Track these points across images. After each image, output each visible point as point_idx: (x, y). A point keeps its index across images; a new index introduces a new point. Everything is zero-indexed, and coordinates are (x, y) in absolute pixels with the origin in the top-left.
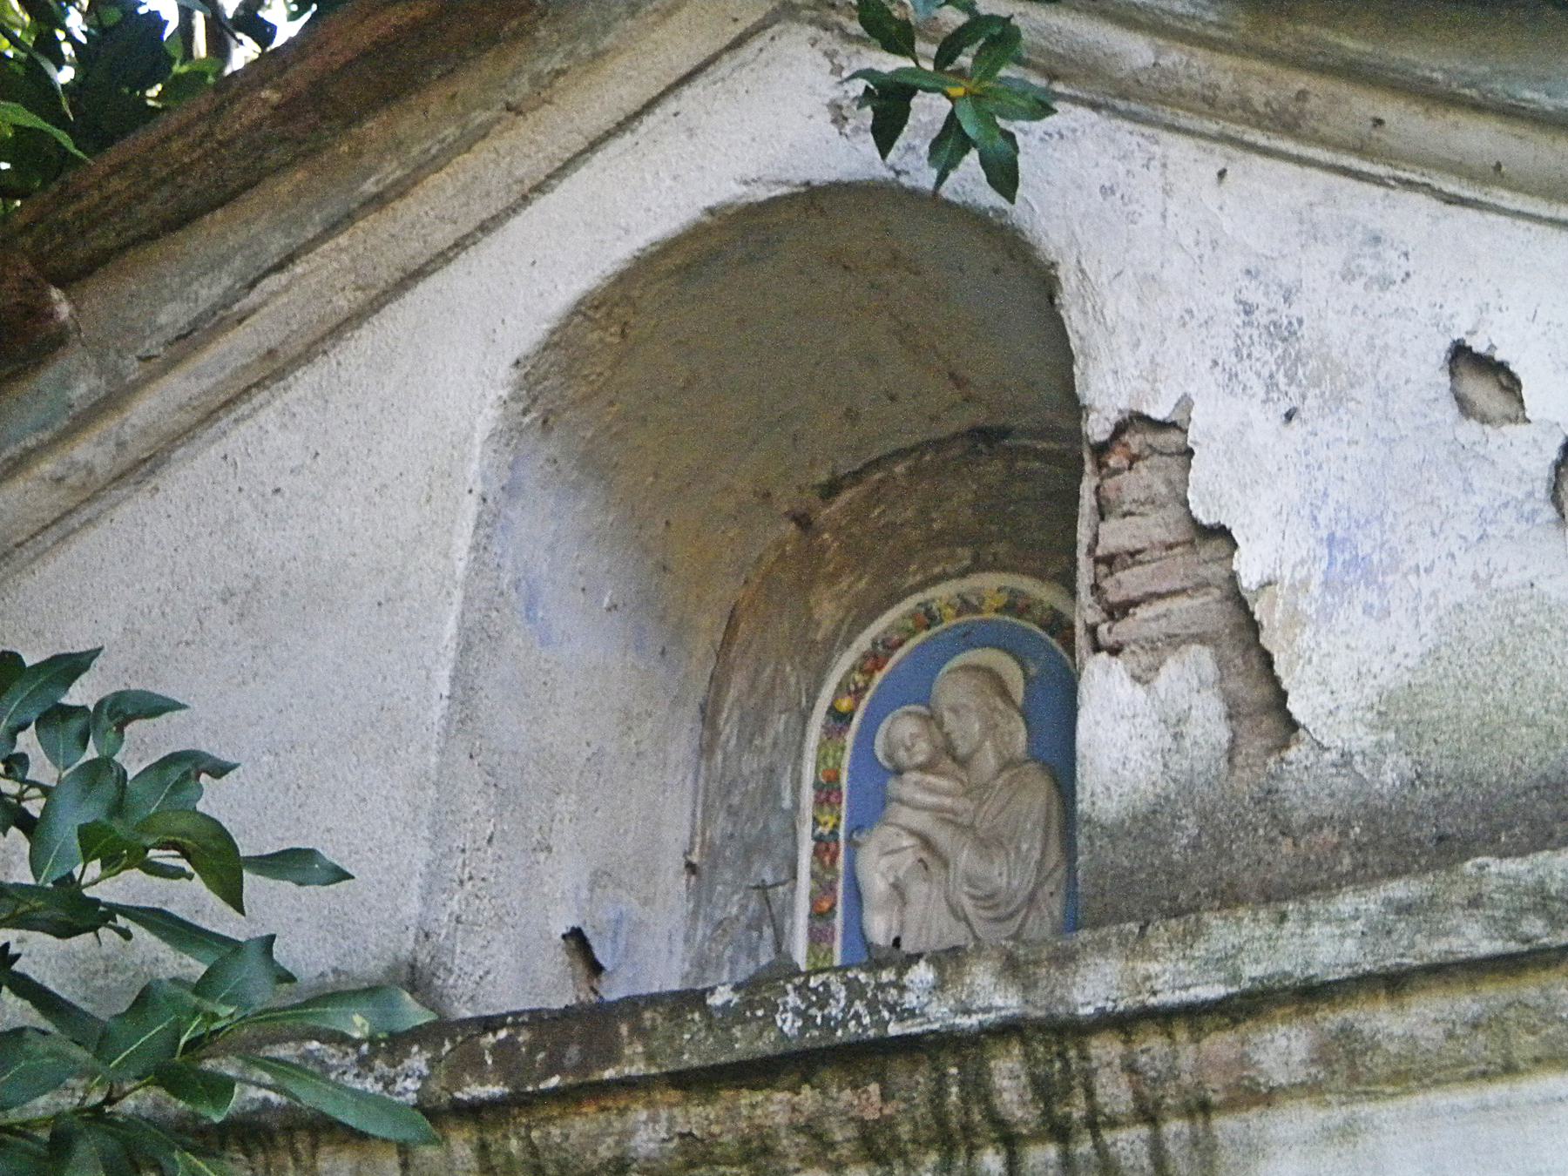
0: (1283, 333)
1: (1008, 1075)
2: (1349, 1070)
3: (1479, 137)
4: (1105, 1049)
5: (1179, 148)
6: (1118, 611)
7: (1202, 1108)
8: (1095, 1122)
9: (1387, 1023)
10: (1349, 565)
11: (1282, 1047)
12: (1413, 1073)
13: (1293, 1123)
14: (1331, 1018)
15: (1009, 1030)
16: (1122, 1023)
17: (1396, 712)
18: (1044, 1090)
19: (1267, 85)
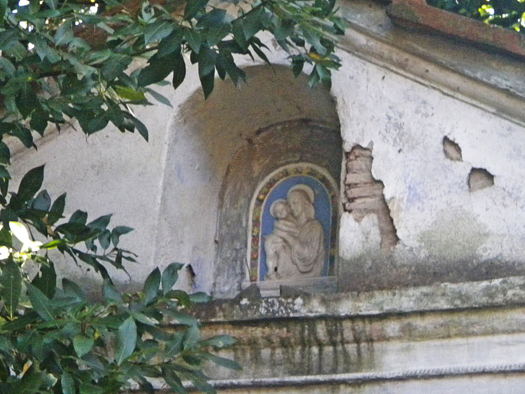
0: (399, 127)
1: (321, 330)
2: (409, 334)
3: (454, 79)
4: (347, 325)
5: (372, 68)
6: (351, 200)
7: (370, 340)
8: (343, 342)
9: (419, 322)
10: (415, 196)
11: (392, 327)
12: (425, 336)
13: (395, 346)
14: (406, 321)
15: (322, 318)
16: (352, 318)
17: (425, 238)
18: (330, 333)
19: (397, 55)
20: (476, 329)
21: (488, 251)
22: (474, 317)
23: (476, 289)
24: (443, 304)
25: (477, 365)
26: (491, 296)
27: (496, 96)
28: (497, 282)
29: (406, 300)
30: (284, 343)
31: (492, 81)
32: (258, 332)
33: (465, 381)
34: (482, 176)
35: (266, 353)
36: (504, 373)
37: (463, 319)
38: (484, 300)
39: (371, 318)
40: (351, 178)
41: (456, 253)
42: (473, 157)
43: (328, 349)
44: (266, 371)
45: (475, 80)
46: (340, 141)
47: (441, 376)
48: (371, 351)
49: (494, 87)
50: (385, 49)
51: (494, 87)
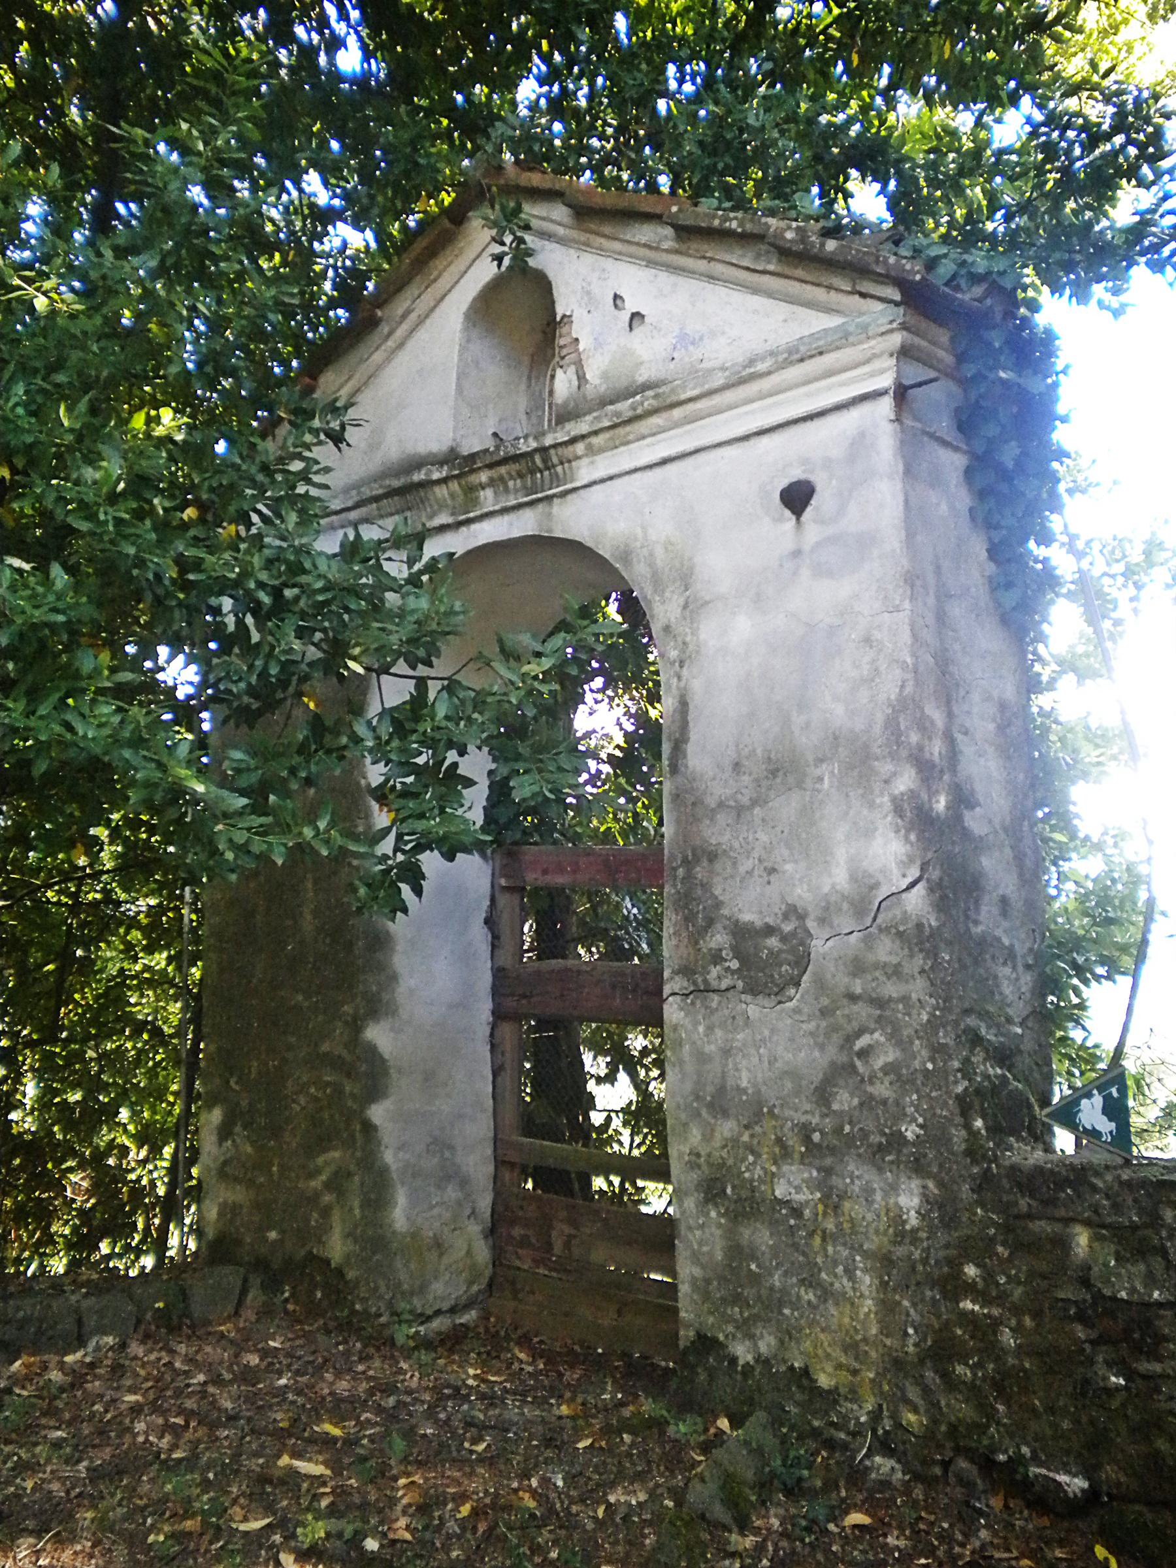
0: (588, 293)
1: (538, 459)
2: (591, 451)
3: (617, 246)
4: (552, 452)
5: (572, 251)
6: (563, 358)
7: (569, 461)
8: (554, 466)
9: (596, 441)
10: (598, 344)
11: (580, 448)
12: (602, 450)
13: (585, 462)
14: (587, 441)
15: (536, 450)
16: (555, 446)
17: (605, 376)
18: (545, 461)
19: (583, 237)
20: (631, 437)
21: (642, 376)
22: (628, 428)
23: (624, 407)
24: (607, 424)
25: (627, 466)
26: (635, 409)
27: (643, 252)
28: (638, 397)
29: (582, 426)
30: (521, 475)
31: (636, 240)
32: (503, 470)
33: (627, 478)
34: (636, 317)
35: (511, 484)
36: (650, 467)
37: (621, 431)
38: (630, 414)
39: (566, 444)
40: (562, 342)
41: (623, 383)
42: (631, 306)
43: (546, 473)
44: (512, 497)
45: (628, 242)
46: (554, 314)
47: (611, 478)
48: (571, 468)
49: (638, 244)
50: (575, 234)
51: (638, 244)
